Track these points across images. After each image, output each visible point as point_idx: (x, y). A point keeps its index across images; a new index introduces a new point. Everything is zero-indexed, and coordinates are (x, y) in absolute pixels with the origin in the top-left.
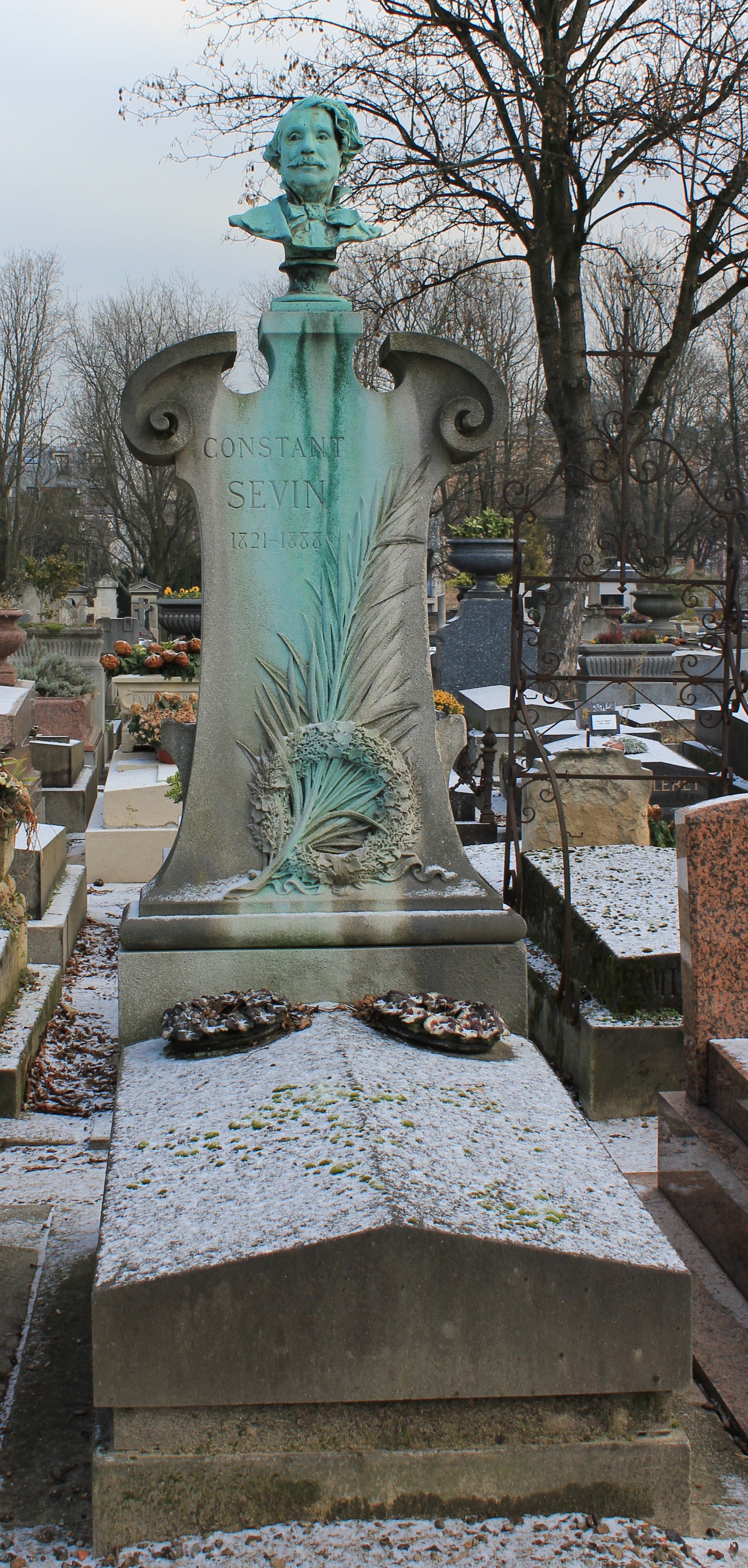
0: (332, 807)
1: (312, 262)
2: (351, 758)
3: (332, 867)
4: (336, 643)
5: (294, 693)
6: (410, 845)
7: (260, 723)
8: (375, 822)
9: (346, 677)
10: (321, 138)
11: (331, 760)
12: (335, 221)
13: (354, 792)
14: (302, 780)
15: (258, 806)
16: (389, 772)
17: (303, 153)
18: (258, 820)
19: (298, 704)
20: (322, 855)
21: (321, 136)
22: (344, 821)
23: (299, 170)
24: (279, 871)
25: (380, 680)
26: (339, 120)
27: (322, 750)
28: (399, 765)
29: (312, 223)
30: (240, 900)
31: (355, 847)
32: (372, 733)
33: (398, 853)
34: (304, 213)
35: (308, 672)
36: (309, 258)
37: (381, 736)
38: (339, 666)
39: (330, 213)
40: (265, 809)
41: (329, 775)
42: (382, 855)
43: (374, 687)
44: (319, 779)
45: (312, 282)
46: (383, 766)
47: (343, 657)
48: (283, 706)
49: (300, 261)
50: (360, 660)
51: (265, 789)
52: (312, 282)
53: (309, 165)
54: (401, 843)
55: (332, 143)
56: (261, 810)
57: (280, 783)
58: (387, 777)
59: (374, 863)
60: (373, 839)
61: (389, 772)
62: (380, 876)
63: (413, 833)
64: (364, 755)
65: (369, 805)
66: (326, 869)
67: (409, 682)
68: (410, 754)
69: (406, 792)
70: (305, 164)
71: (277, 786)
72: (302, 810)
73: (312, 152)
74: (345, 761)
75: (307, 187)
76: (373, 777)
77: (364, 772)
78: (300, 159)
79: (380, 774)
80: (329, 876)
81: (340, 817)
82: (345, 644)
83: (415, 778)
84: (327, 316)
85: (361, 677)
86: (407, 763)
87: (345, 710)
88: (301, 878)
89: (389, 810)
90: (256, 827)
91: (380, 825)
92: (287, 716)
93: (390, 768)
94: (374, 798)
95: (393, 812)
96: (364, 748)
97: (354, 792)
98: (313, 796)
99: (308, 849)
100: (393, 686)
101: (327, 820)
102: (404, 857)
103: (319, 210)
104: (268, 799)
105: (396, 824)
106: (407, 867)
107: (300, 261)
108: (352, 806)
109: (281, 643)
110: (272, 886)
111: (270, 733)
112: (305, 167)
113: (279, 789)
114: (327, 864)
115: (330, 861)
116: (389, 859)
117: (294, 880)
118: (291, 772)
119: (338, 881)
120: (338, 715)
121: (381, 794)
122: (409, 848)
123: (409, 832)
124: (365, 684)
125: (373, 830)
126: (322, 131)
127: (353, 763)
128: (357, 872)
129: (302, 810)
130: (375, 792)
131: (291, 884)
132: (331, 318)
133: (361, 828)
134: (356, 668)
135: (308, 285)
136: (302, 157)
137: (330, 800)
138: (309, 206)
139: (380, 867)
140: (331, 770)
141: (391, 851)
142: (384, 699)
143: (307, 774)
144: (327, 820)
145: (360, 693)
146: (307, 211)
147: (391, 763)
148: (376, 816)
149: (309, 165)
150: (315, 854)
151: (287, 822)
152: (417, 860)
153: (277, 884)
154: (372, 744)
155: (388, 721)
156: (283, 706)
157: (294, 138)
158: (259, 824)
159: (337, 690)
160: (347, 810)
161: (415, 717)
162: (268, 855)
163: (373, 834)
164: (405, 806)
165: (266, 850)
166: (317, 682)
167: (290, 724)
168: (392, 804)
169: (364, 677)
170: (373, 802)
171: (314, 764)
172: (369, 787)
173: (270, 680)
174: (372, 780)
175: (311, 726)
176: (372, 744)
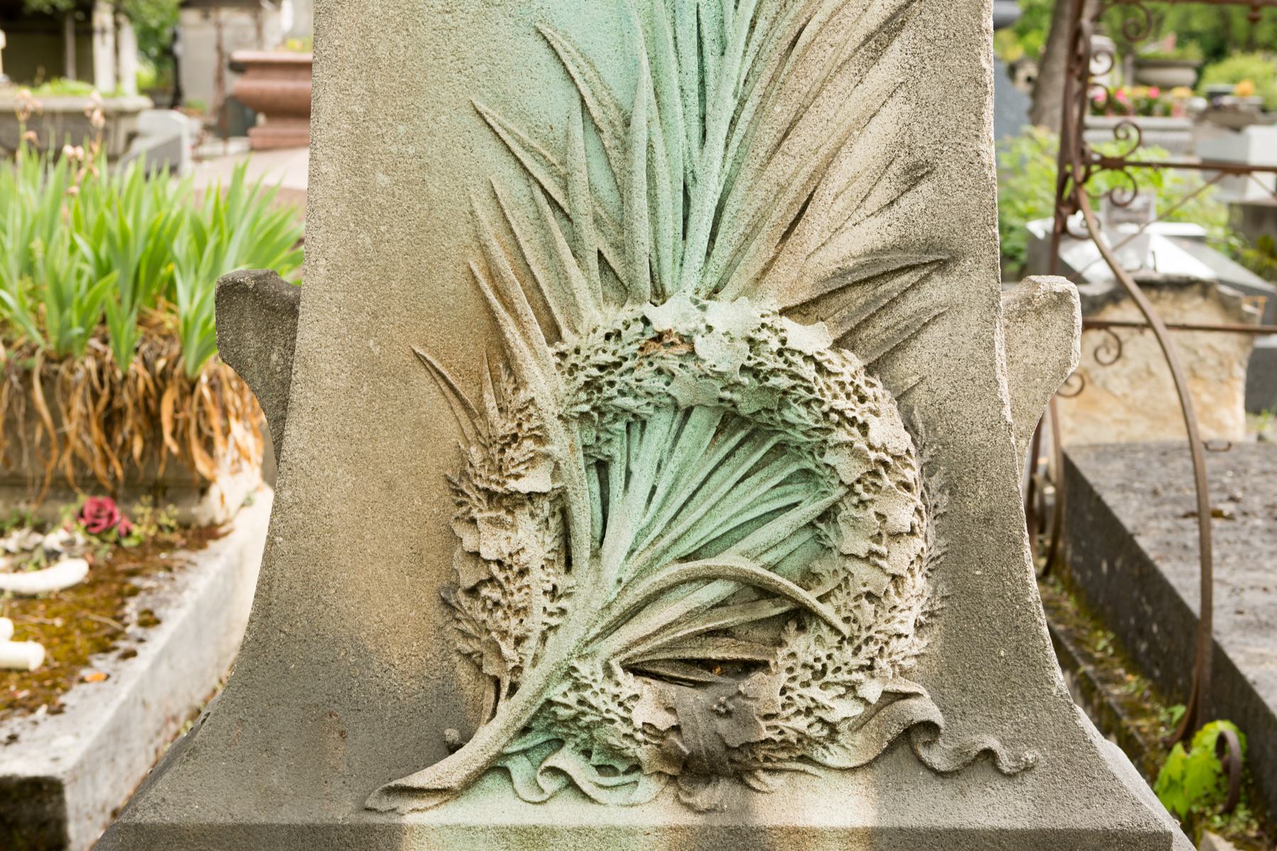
0: (685, 547)
2: (746, 409)
3: (676, 729)
4: (710, 61)
5: (582, 207)
6: (907, 664)
7: (485, 299)
8: (809, 598)
9: (737, 162)
11: (688, 412)
13: (752, 506)
14: (602, 467)
15: (469, 542)
16: (858, 455)
18: (468, 581)
19: (593, 241)
20: (647, 689)
22: (718, 590)
24: (526, 730)
25: (838, 178)
27: (659, 384)
28: (887, 431)
30: (410, 819)
31: (748, 667)
32: (810, 338)
33: (872, 690)
35: (625, 148)
37: (838, 344)
38: (718, 130)
40: (486, 553)
41: (679, 456)
42: (824, 697)
43: (824, 195)
44: (650, 468)
46: (840, 435)
47: (731, 104)
48: (550, 249)
50: (781, 112)
51: (490, 495)
54: (882, 663)
56: (477, 554)
57: (536, 481)
58: (850, 470)
59: (801, 723)
60: (802, 645)
61: (858, 455)
62: (818, 753)
63: (919, 626)
64: (783, 404)
65: (794, 544)
66: (661, 735)
67: (925, 187)
68: (920, 398)
69: (902, 514)
71: (524, 486)
72: (596, 555)
74: (729, 419)
76: (808, 464)
77: (781, 448)
79: (830, 458)
80: (667, 756)
81: (710, 579)
82: (736, 66)
83: (929, 469)
85: (783, 166)
86: (910, 426)
87: (731, 266)
88: (587, 753)
89: (854, 566)
90: (465, 601)
91: (826, 610)
92: (562, 277)
93: (860, 444)
94: (811, 525)
95: (861, 571)
96: (783, 382)
97: (752, 506)
98: (629, 516)
99: (608, 669)
100: (881, 195)
101: (672, 587)
102: (892, 697)
104: (496, 522)
105: (868, 607)
106: (896, 729)
108: (745, 545)
109: (546, 56)
110: (506, 772)
111: (511, 330)
113: (531, 496)
114: (663, 721)
115: (671, 710)
116: (844, 710)
117: (566, 759)
118: (563, 443)
119: (689, 769)
120: (712, 280)
121: (828, 515)
122: (903, 672)
123: (908, 629)
124: (797, 184)
125: (801, 616)
127: (754, 421)
128: (750, 746)
129: (596, 555)
130: (811, 508)
131: (555, 771)
133: (770, 610)
134: (769, 140)
137: (678, 529)
139: (817, 732)
140: (683, 441)
141: (851, 687)
142: (847, 234)
143: (616, 450)
144: (672, 587)
145: (780, 215)
147: (864, 428)
148: (809, 578)
150: (631, 684)
151: (553, 593)
152: (925, 708)
153: (519, 768)
154: (808, 371)
155: (858, 297)
156: (550, 249)
158: (473, 592)
159: (711, 207)
160: (730, 559)
161: (938, 290)
162: (497, 682)
163: (801, 628)
164: (900, 557)
165: (490, 670)
166: (651, 177)
167: (571, 304)
168: (862, 547)
169: (791, 168)
170: (807, 535)
171: (637, 423)
172: (797, 492)
173: (511, 170)
174: (807, 473)
175: (629, 312)
176: (808, 371)
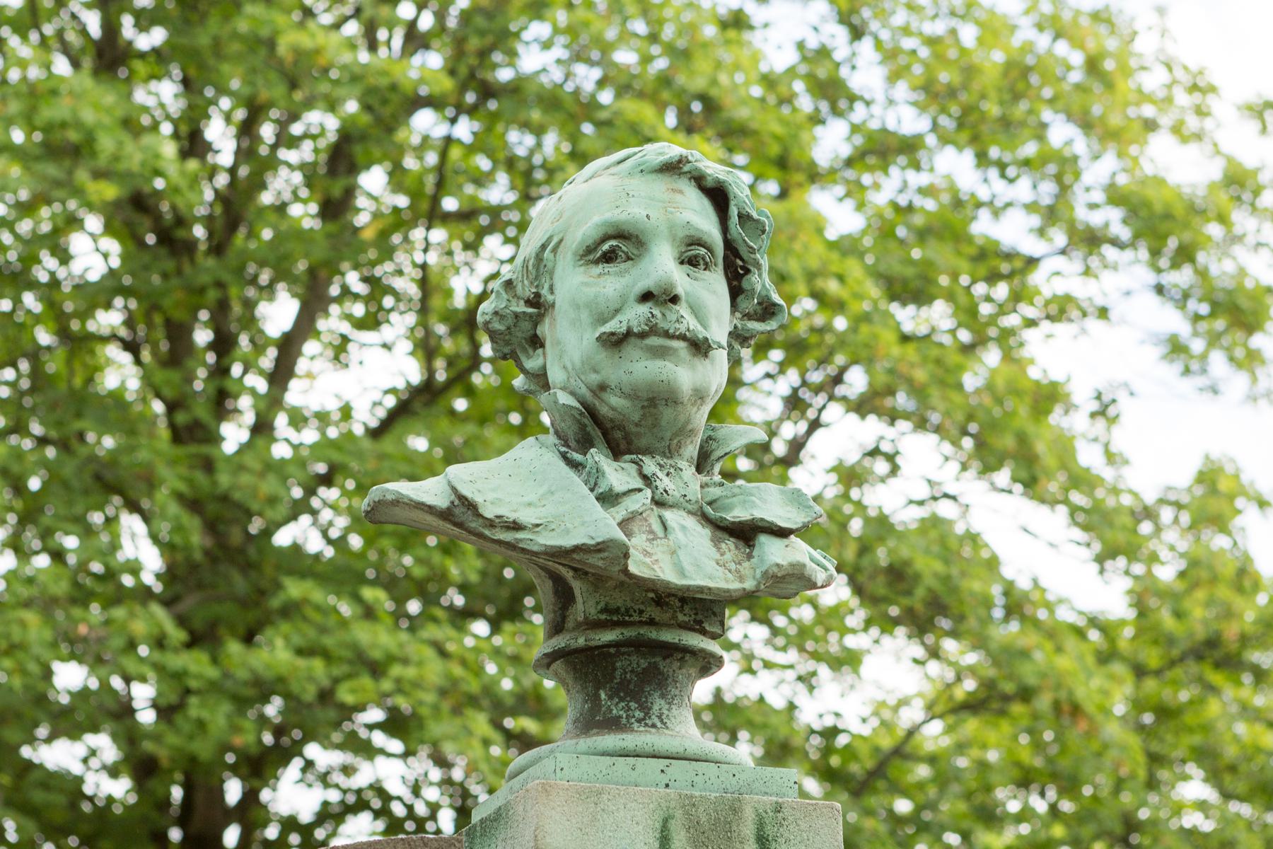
1: (668, 636)
10: (692, 262)
12: (738, 514)
17: (646, 297)
21: (692, 255)
23: (632, 350)
26: (744, 218)
29: (668, 515)
34: (638, 483)
36: (652, 622)
39: (715, 492)
45: (658, 704)
49: (630, 633)
52: (658, 704)
53: (667, 335)
55: (711, 289)
70: (653, 330)
73: (675, 299)
75: (657, 400)
78: (636, 315)
84: (735, 809)
103: (683, 480)
107: (630, 633)
112: (654, 341)
126: (699, 243)
132: (749, 814)
135: (646, 710)
136: (644, 309)
138: (650, 466)
146: (647, 479)
149: (667, 335)
157: (609, 257)
